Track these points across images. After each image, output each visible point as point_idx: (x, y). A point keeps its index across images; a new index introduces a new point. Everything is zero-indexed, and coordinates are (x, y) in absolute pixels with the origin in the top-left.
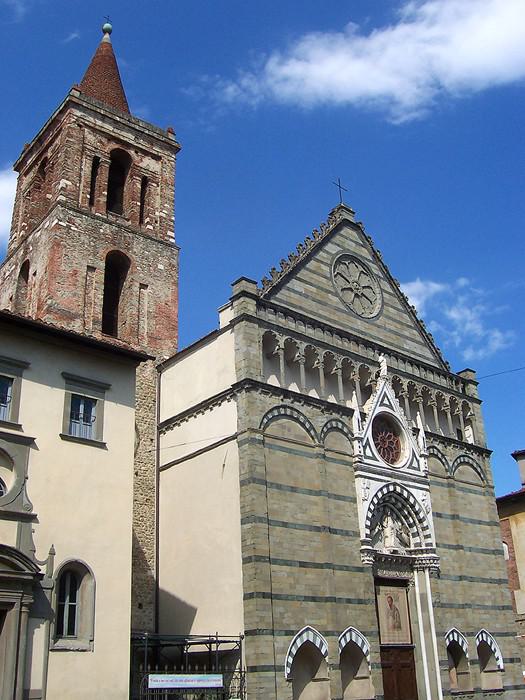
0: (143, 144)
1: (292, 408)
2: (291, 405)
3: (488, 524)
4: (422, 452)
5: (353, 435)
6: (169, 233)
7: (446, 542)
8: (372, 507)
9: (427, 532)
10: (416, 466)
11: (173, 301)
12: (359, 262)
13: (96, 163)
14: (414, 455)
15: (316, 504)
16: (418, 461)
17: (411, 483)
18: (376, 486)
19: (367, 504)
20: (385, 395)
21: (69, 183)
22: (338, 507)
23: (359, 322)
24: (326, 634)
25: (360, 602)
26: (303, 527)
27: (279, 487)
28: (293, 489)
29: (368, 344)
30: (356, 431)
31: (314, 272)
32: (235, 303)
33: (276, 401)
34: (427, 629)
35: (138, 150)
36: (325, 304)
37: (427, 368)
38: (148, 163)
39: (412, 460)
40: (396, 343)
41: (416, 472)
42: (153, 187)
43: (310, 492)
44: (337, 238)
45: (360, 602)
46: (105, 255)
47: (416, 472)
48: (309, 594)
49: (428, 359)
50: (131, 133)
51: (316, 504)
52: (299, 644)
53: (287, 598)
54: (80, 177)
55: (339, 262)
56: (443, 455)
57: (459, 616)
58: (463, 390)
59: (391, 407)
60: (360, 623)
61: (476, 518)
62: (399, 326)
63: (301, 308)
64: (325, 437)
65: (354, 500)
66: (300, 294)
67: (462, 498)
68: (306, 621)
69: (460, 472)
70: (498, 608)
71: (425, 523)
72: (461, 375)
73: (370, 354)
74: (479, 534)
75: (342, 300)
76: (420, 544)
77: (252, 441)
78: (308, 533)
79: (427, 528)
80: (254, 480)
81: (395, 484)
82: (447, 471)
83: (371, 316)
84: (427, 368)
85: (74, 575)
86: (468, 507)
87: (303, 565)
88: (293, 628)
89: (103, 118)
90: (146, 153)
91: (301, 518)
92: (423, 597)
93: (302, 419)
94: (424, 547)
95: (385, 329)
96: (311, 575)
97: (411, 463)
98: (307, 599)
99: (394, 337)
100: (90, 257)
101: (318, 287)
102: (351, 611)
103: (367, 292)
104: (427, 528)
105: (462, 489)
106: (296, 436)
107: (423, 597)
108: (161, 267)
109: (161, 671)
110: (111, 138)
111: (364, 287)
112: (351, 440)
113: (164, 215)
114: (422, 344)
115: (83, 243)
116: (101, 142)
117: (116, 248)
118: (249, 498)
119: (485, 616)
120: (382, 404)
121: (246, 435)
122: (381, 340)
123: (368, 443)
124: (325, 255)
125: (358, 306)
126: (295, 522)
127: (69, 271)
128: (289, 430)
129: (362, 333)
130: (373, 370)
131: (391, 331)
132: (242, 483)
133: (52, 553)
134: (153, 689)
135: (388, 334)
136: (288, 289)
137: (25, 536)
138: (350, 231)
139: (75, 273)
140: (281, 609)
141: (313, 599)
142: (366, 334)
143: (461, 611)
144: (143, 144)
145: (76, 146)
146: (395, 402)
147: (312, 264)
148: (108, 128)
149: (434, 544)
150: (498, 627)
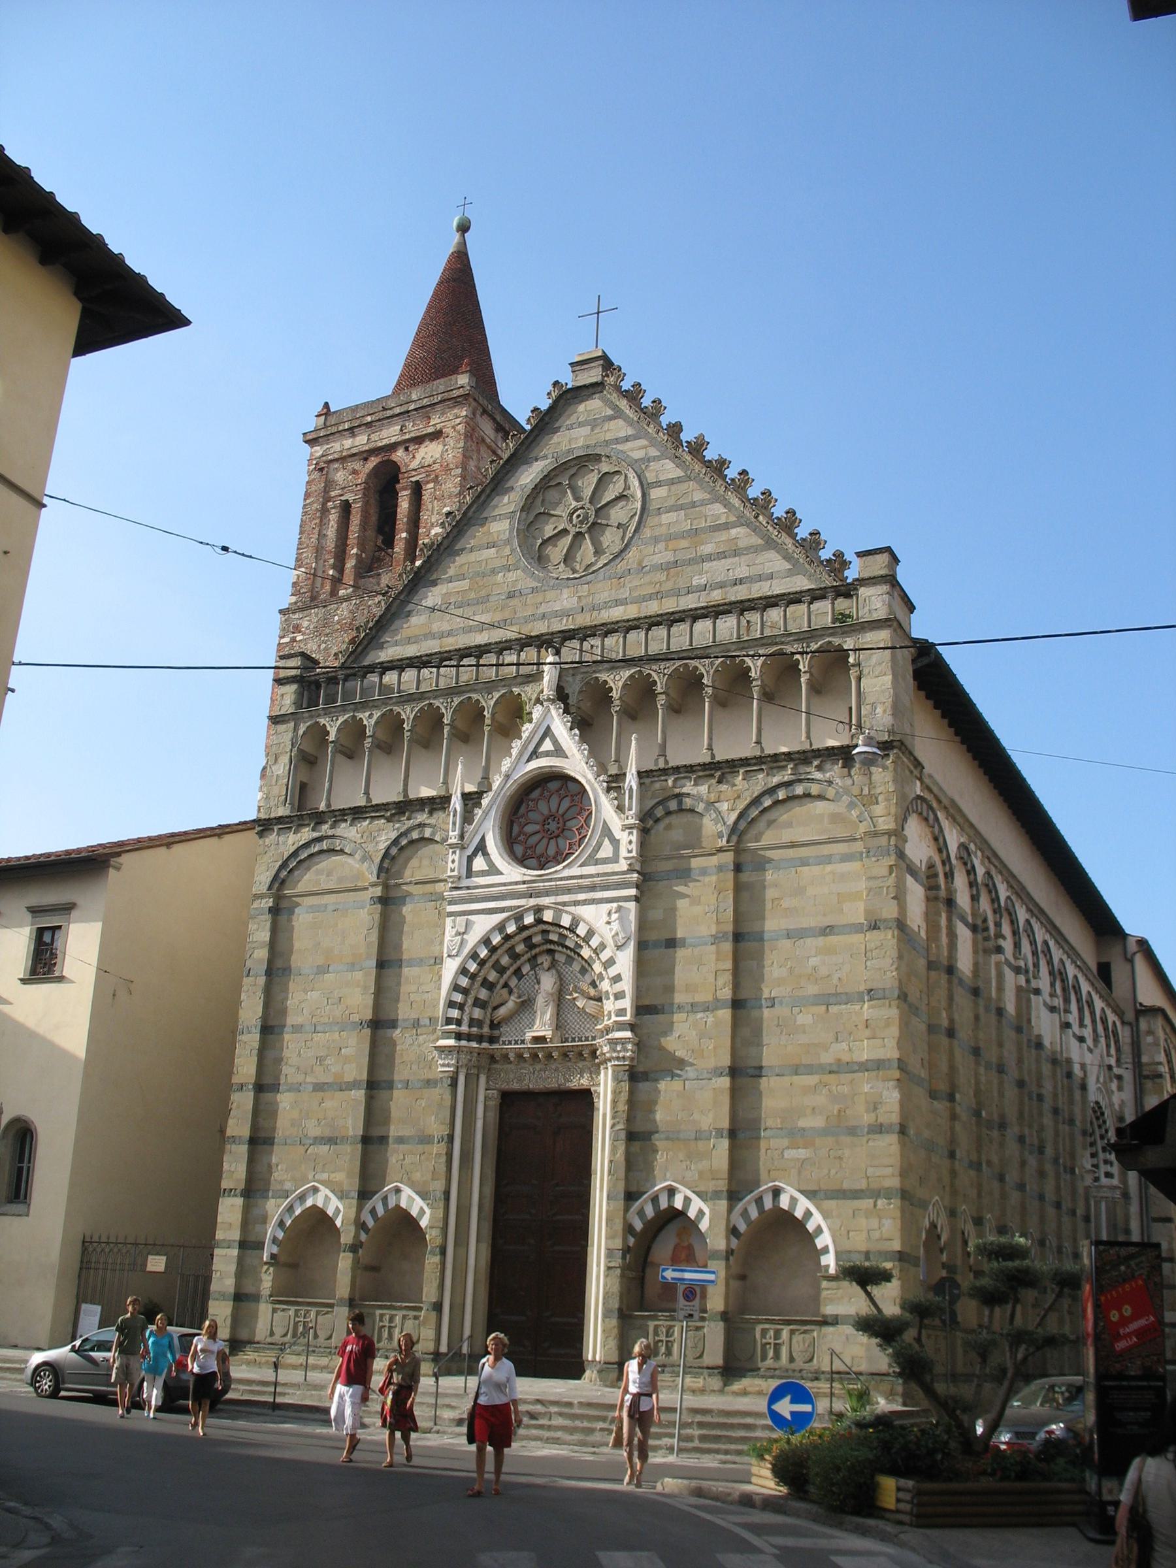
0: (414, 428)
2: (330, 833)
3: (856, 928)
9: (618, 987)
10: (601, 854)
16: (615, 843)
17: (581, 897)
33: (306, 834)
35: (406, 444)
38: (430, 452)
48: (327, 1133)
50: (390, 425)
57: (689, 1157)
59: (559, 752)
60: (417, 1176)
62: (684, 543)
68: (310, 1177)
70: (852, 1131)
71: (613, 972)
81: (538, 910)
88: (288, 1186)
90: (419, 440)
104: (617, 979)
106: (340, 880)
110: (365, 456)
119: (790, 1154)
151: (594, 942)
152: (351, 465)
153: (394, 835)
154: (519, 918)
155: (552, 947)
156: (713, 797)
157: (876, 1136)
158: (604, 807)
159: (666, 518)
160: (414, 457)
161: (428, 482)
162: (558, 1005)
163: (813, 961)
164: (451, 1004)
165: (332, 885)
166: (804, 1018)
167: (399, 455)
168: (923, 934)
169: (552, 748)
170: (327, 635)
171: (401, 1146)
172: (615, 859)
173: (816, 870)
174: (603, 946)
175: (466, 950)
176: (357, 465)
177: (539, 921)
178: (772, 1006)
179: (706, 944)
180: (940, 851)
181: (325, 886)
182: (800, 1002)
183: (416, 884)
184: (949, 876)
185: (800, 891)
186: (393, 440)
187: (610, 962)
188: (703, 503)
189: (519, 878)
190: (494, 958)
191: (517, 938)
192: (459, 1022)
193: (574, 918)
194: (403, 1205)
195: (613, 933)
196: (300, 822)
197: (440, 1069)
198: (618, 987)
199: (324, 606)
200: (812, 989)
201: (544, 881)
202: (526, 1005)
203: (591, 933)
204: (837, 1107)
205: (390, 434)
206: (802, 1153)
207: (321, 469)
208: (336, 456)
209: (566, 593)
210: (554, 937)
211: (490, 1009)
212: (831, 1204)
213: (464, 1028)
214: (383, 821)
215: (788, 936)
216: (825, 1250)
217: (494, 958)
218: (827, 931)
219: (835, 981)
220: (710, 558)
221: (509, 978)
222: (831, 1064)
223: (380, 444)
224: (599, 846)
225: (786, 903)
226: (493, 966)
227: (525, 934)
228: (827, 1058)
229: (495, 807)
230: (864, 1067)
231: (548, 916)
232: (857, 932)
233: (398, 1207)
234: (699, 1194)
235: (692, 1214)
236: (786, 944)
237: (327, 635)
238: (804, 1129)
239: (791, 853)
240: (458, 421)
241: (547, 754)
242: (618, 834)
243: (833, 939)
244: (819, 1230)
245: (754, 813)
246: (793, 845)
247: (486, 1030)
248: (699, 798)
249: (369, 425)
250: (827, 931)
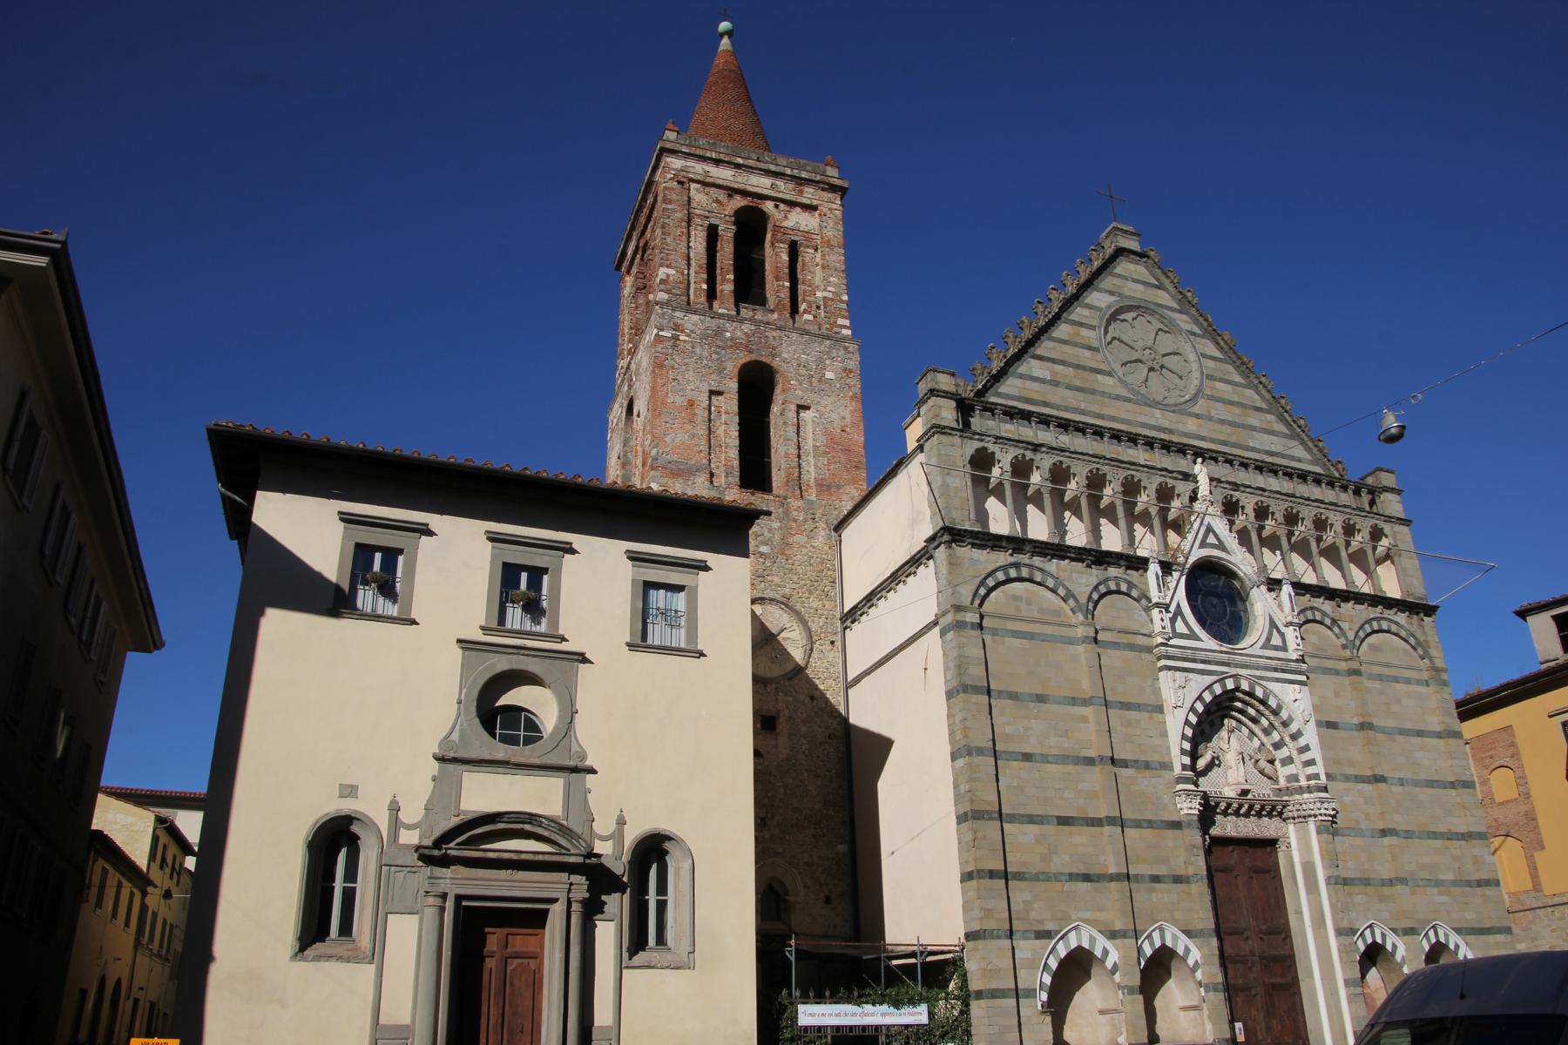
1: (1031, 566)
3: (1439, 735)
4: (1290, 619)
5: (1149, 600)
6: (840, 321)
7: (1350, 771)
8: (1193, 719)
9: (1307, 756)
11: (854, 424)
12: (1153, 313)
13: (712, 235)
14: (1273, 625)
15: (1085, 719)
16: (1282, 635)
18: (1198, 683)
19: (1181, 715)
20: (1210, 529)
21: (671, 272)
22: (1128, 723)
23: (1158, 413)
24: (1113, 935)
25: (1178, 879)
26: (1063, 759)
27: (1014, 696)
28: (1041, 699)
29: (1182, 450)
30: (1155, 596)
31: (1065, 342)
32: (923, 410)
33: (1003, 558)
34: (1319, 923)
36: (1093, 392)
37: (1303, 476)
38: (798, 220)
39: (1270, 634)
40: (1233, 439)
41: (1281, 654)
42: (807, 255)
43: (1073, 701)
44: (1107, 282)
45: (1178, 879)
46: (736, 370)
47: (1281, 654)
49: (1299, 460)
51: (1085, 719)
52: (1062, 951)
53: (1036, 878)
54: (689, 259)
55: (1114, 317)
56: (1334, 621)
57: (1382, 899)
58: (1372, 503)
59: (1221, 546)
60: (1179, 915)
61: (1408, 725)
62: (1237, 410)
63: (1046, 404)
64: (1095, 608)
65: (1159, 709)
66: (1043, 381)
67: (1381, 693)
68: (1074, 916)
69: (1372, 647)
70: (1469, 883)
71: (1302, 742)
72: (1370, 481)
73: (1183, 464)
74: (1419, 754)
75: (1121, 381)
76: (1295, 778)
77: (959, 626)
78: (1071, 768)
79: (1306, 748)
80: (965, 689)
82: (1344, 647)
83: (1183, 400)
84: (1303, 476)
86: (1395, 708)
87: (1063, 821)
88: (1050, 926)
89: (717, 162)
90: (792, 204)
91: (1055, 745)
92: (1309, 869)
93: (1050, 583)
94: (1303, 782)
95: (1210, 419)
96: (1080, 837)
97: (1268, 639)
98: (1073, 877)
99: (1227, 429)
100: (714, 377)
101: (1077, 367)
102: (1164, 895)
103: (1170, 362)
104: (1306, 748)
105: (1380, 678)
106: (1041, 611)
107: (1309, 869)
108: (829, 375)
109: (820, 999)
110: (732, 192)
111: (1164, 355)
112: (1147, 610)
113: (830, 295)
114: (1286, 436)
115: (700, 358)
116: (718, 201)
117: (753, 357)
118: (959, 717)
120: (1203, 545)
121: (949, 618)
122: (1203, 438)
123: (1179, 611)
124: (1086, 312)
125: (1156, 387)
126: (1045, 751)
127: (680, 401)
128: (1029, 603)
129: (1165, 430)
130: (1183, 488)
131: (1222, 422)
132: (950, 695)
133: (621, 822)
134: (806, 1028)
135: (1218, 427)
136: (1021, 376)
137: (576, 799)
138: (1132, 267)
139: (691, 403)
140: (1027, 896)
141: (1087, 878)
142: (1171, 431)
143: (1386, 890)
144: (785, 189)
145: (679, 215)
146: (1231, 541)
147: (1062, 330)
148: (724, 174)
149: (1323, 777)
150: (1470, 918)
151: (1284, 715)
152: (715, 193)
153: (1094, 581)
154: (1221, 681)
158: (1261, 604)
159: (1219, 385)
160: (786, 217)
161: (808, 247)
165: (1036, 615)
167: (769, 206)
169: (1208, 541)
170: (719, 347)
171: (1157, 885)
172: (1284, 648)
174: (1291, 719)
175: (1188, 705)
176: (721, 195)
177: (1237, 689)
179: (1352, 730)
181: (1024, 613)
182: (1417, 783)
183: (1119, 632)
185: (1398, 701)
186: (765, 192)
188: (1240, 385)
189: (1217, 648)
193: (1264, 691)
194: (1169, 943)
195: (1301, 710)
196: (997, 543)
197: (1186, 811)
198: (1307, 756)
199: (712, 318)
200: (1423, 776)
201: (1235, 654)
203: (1280, 707)
205: (761, 183)
206: (1445, 899)
207: (680, 183)
208: (699, 178)
214: (1080, 564)
219: (1434, 771)
220: (1254, 429)
223: (750, 189)
228: (1442, 828)
229: (1184, 578)
231: (1245, 686)
232: (1437, 738)
233: (1164, 946)
234: (1394, 930)
235: (1389, 947)
237: (719, 347)
238: (1442, 880)
240: (835, 206)
241: (1212, 546)
242: (1283, 629)
246: (1388, 665)
248: (1324, 614)
249: (738, 166)
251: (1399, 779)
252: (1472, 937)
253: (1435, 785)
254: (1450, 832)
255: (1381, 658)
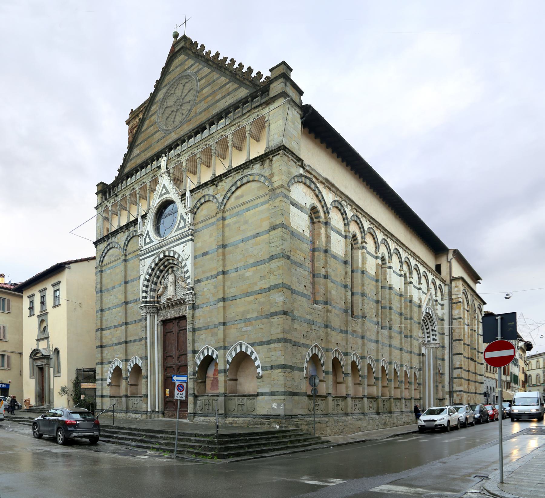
70: (267, 317)
71: (185, 269)
79: (187, 271)
85: (57, 351)
155: (171, 265)
156: (215, 193)
157: (274, 317)
162: (175, 287)
163: (250, 250)
164: (143, 292)
166: (249, 273)
168: (307, 233)
173: (252, 212)
178: (238, 271)
180: (320, 201)
182: (246, 267)
184: (327, 212)
185: (246, 222)
187: (185, 265)
190: (154, 272)
191: (160, 264)
192: (146, 298)
200: (251, 261)
202: (166, 288)
203: (179, 256)
204: (261, 308)
206: (249, 328)
209: (173, 134)
210: (171, 261)
211: (156, 292)
212: (260, 348)
213: (148, 299)
215: (243, 241)
216: (258, 367)
217: (154, 272)
218: (257, 235)
221: (161, 280)
222: (258, 290)
224: (180, 222)
225: (241, 229)
226: (155, 276)
227: (162, 262)
228: (257, 288)
230: (270, 289)
236: (242, 245)
238: (249, 319)
239: (243, 207)
243: (258, 239)
244: (256, 359)
245: (229, 194)
247: (156, 299)
250: (257, 235)
251: (236, 268)
252: (261, 346)
253: (259, 264)
254: (261, 289)
255: (242, 201)
